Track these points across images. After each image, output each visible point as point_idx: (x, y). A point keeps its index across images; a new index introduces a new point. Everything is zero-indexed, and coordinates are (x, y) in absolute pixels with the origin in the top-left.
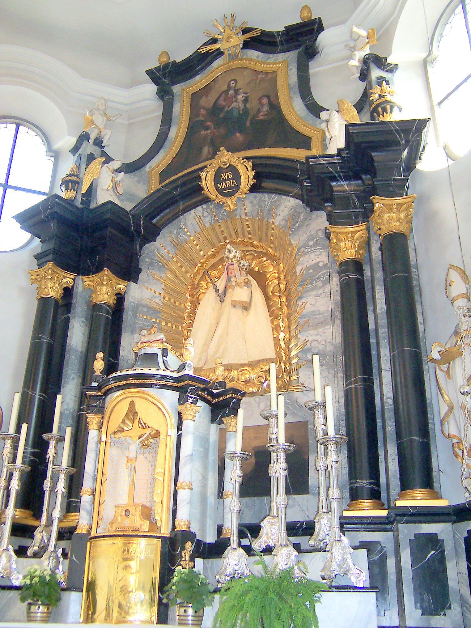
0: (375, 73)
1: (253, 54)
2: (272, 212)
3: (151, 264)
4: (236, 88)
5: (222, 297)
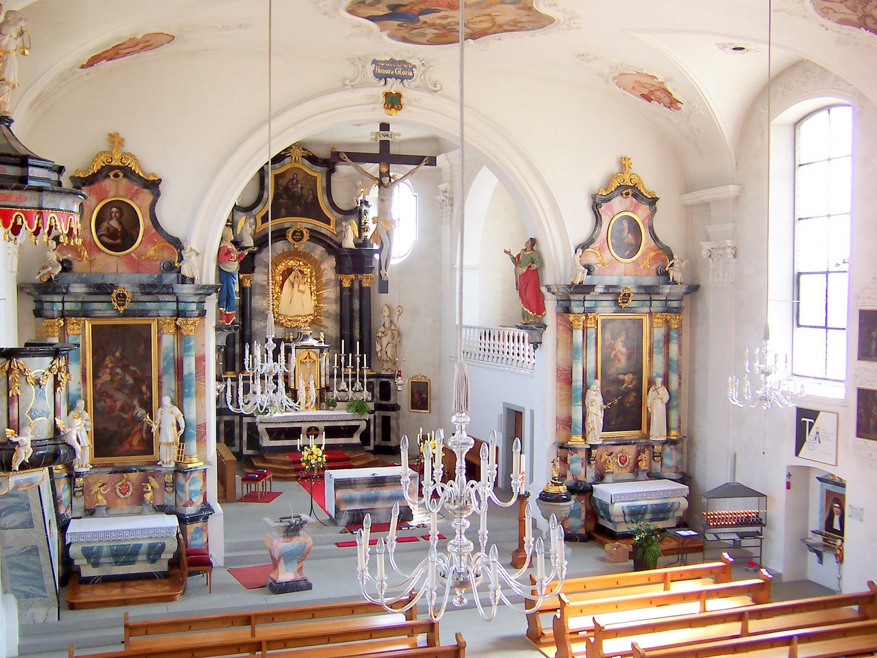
0: (364, 208)
1: (306, 162)
2: (312, 251)
3: (260, 265)
4: (298, 179)
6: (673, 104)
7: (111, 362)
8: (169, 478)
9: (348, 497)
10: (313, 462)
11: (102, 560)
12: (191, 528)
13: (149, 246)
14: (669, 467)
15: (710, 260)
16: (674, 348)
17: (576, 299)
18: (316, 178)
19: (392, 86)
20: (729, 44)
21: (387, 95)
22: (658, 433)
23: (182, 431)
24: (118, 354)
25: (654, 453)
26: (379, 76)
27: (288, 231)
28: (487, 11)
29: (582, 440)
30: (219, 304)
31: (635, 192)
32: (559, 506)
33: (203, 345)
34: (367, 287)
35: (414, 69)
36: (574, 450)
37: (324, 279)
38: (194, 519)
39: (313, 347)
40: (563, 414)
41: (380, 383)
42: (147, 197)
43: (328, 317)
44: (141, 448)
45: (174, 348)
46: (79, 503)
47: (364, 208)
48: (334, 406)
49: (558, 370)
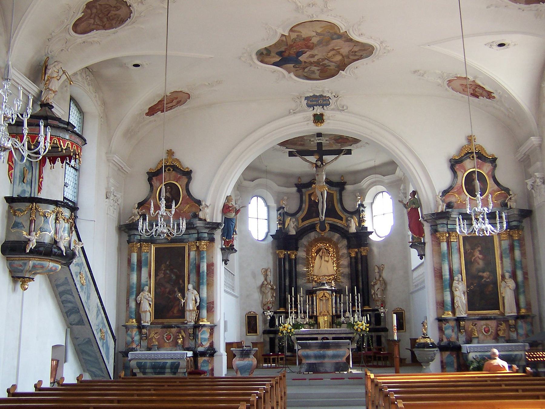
0: (362, 209)
3: (301, 246)
5: (321, 257)
6: (489, 95)
7: (165, 267)
8: (191, 331)
9: (305, 353)
10: (284, 332)
11: (147, 371)
12: (201, 360)
13: (185, 205)
14: (522, 335)
15: (533, 191)
16: (517, 253)
17: (439, 223)
18: (333, 194)
19: (317, 110)
20: (492, 42)
21: (315, 115)
22: (510, 309)
23: (198, 304)
24: (168, 263)
25: (510, 325)
26: (309, 106)
27: (316, 225)
28: (330, 47)
29: (451, 314)
30: (223, 235)
31: (481, 156)
32: (425, 350)
33: (213, 257)
34: (364, 255)
35: (330, 100)
36: (446, 320)
37: (340, 254)
38: (203, 354)
39: (326, 289)
40: (440, 299)
41: (375, 315)
42: (185, 180)
43: (344, 276)
44: (178, 315)
45: (196, 259)
46: (144, 343)
47: (362, 209)
48: (340, 326)
49: (435, 270)
